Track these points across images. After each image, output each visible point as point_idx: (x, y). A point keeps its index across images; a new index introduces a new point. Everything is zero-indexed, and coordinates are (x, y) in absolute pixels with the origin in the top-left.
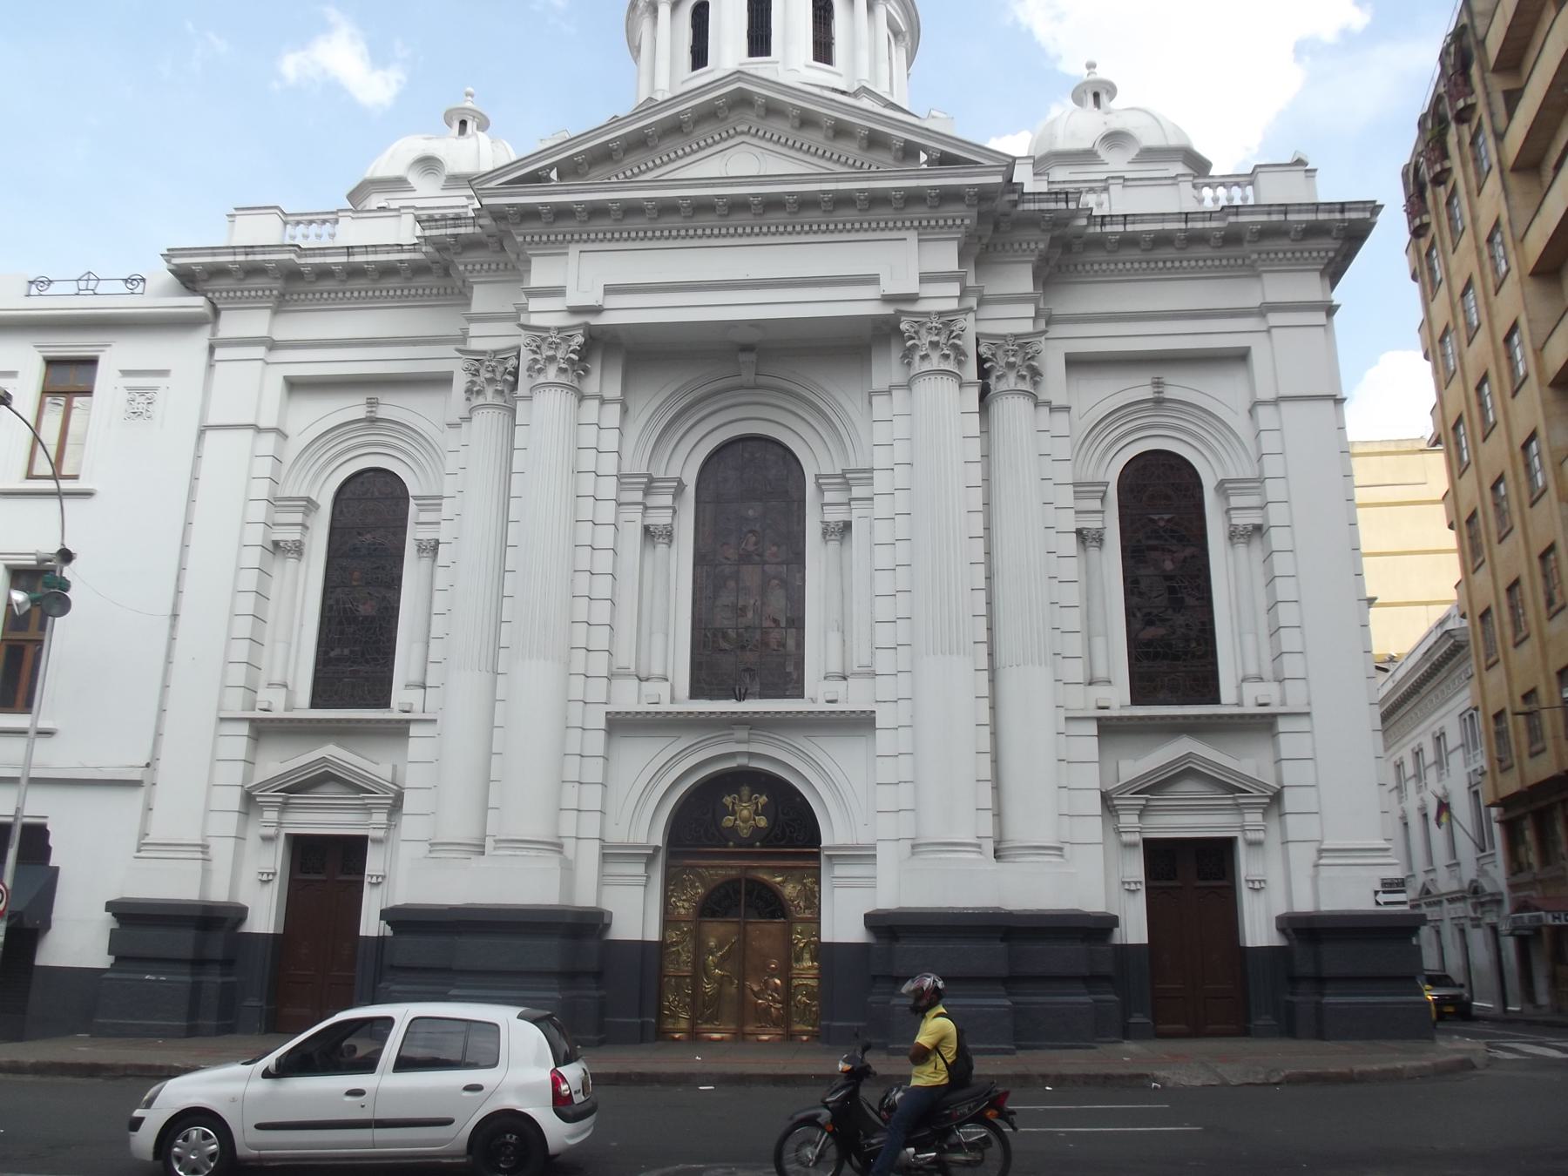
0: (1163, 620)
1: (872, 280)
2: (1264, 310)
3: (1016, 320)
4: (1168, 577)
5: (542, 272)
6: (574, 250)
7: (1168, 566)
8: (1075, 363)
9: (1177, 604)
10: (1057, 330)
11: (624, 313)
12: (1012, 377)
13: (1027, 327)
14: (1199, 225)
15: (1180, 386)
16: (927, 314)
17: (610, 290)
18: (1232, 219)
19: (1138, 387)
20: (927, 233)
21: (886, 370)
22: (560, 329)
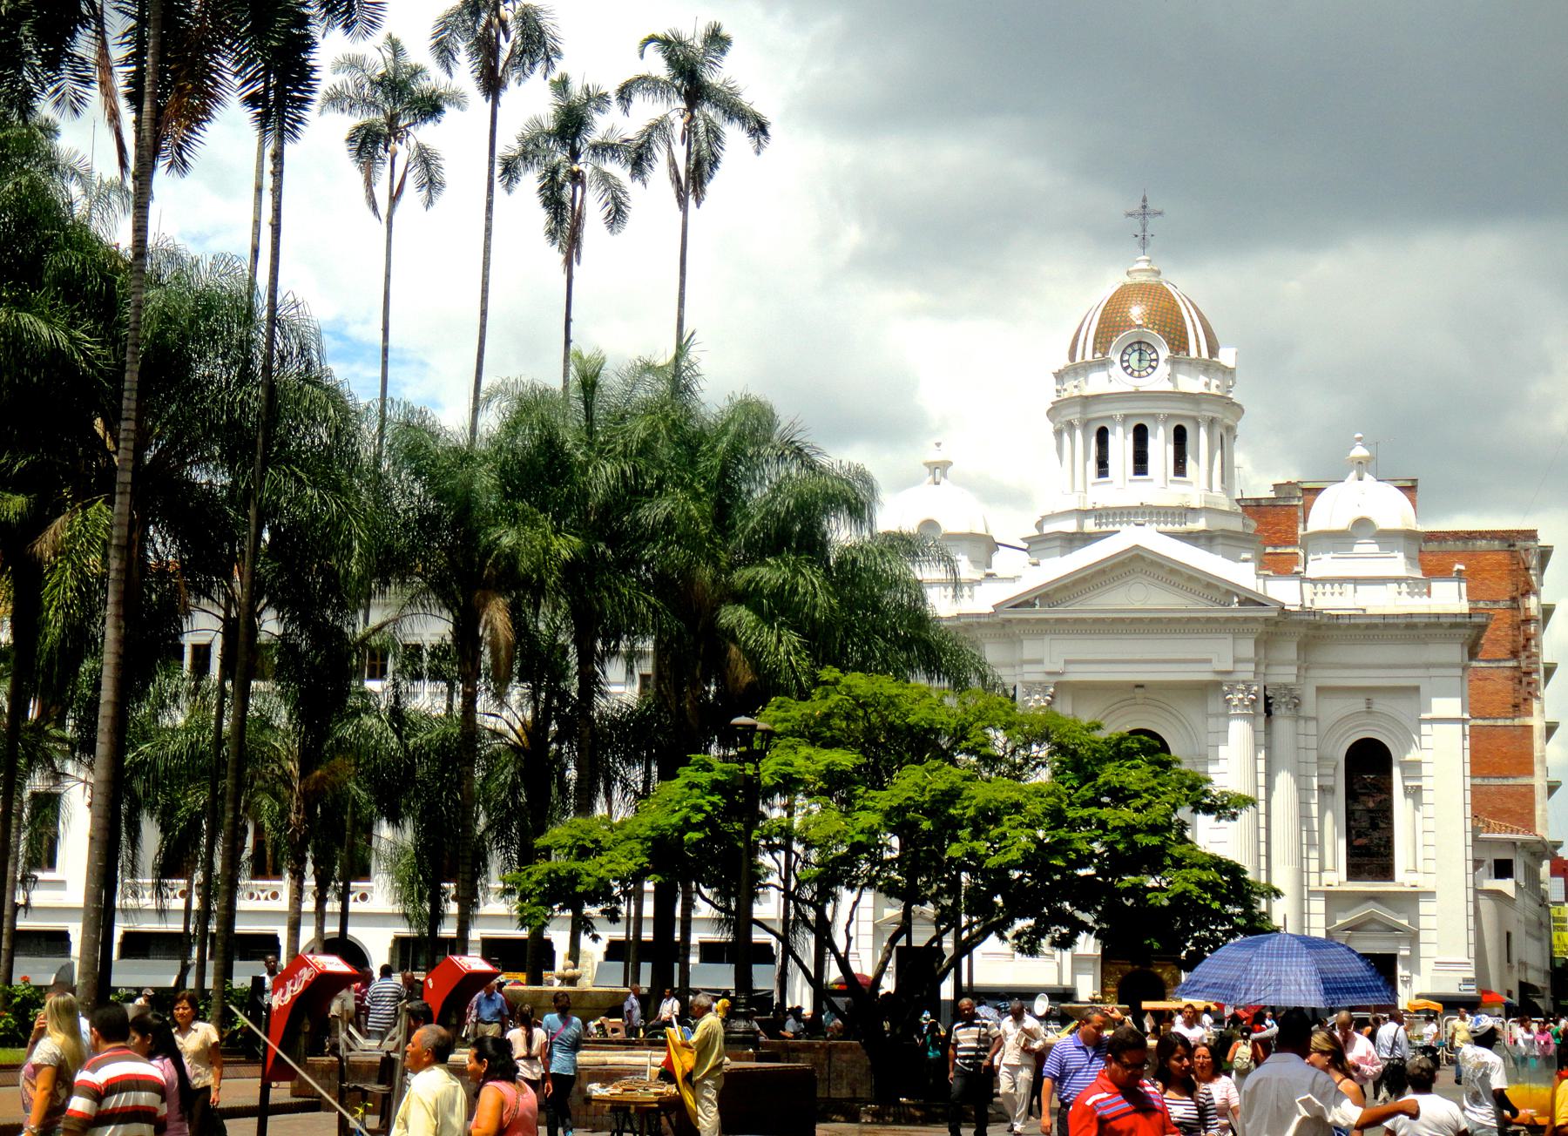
0: (1367, 835)
1: (1209, 661)
2: (1428, 666)
3: (1285, 674)
4: (1369, 811)
5: (1030, 649)
6: (1047, 638)
7: (1371, 805)
8: (1320, 690)
9: (1374, 826)
10: (1313, 673)
11: (1077, 675)
12: (1283, 707)
13: (1293, 679)
14: (1391, 621)
15: (1380, 704)
16: (1238, 682)
17: (1067, 662)
18: (1409, 620)
19: (1359, 704)
20: (1236, 635)
21: (1215, 705)
22: (1040, 683)
